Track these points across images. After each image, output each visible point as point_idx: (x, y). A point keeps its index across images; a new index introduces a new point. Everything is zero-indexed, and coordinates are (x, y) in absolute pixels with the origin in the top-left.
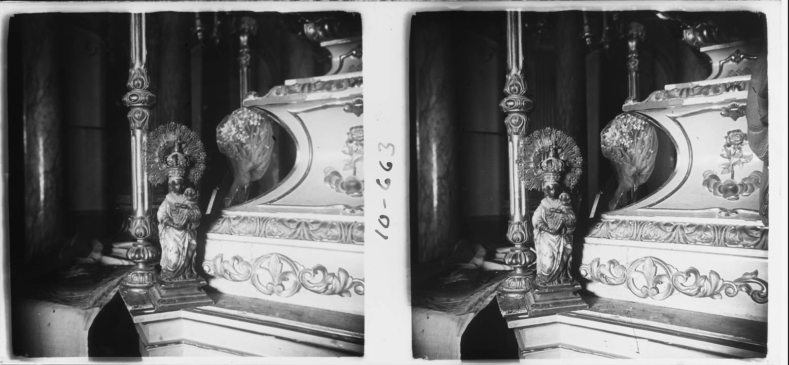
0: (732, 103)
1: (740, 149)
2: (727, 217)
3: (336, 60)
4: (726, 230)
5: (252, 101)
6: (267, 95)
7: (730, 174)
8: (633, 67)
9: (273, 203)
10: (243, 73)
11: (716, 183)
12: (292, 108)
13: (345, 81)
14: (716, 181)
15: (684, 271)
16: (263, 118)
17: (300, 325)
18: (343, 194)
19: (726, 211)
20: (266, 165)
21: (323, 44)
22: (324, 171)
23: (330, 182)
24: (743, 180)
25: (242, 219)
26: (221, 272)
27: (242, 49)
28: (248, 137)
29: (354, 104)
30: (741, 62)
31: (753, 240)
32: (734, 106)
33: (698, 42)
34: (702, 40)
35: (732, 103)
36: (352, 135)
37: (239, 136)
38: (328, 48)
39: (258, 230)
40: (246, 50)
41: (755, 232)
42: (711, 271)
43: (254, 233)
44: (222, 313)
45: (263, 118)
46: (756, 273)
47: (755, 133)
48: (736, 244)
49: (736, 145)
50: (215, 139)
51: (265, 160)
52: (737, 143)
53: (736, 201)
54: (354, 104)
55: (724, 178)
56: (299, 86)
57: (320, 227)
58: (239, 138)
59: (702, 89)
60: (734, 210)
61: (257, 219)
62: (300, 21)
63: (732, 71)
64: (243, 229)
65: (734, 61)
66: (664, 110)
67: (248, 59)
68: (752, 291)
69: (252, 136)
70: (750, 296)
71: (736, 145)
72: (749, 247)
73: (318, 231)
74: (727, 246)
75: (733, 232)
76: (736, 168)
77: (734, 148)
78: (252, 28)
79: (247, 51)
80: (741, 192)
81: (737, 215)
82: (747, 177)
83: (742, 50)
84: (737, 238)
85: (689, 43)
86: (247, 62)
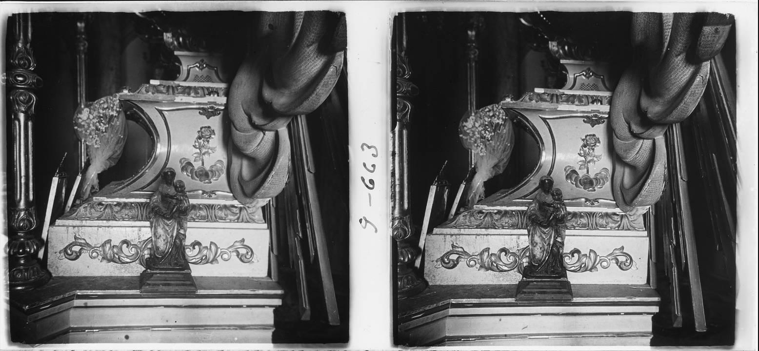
0: (594, 114)
1: (593, 149)
2: (593, 206)
3: (571, 77)
4: (596, 217)
5: (509, 103)
6: (521, 99)
7: (586, 170)
8: (472, 56)
9: (527, 198)
10: (471, 67)
11: (576, 177)
12: (543, 114)
13: (584, 97)
14: (576, 176)
15: (569, 252)
16: (507, 118)
17: (581, 300)
18: (582, 189)
19: (590, 201)
20: (507, 162)
21: (562, 61)
22: (565, 170)
23: (571, 179)
24: (595, 175)
25: (503, 213)
26: (488, 264)
27: (469, 43)
28: (493, 134)
29: (592, 117)
30: (590, 78)
31: (616, 224)
32: (595, 116)
33: (560, 55)
34: (563, 53)
35: (594, 114)
36: (587, 141)
37: (485, 133)
38: (565, 65)
39: (520, 222)
40: (474, 44)
41: (616, 217)
42: (590, 250)
43: (517, 226)
44: (496, 303)
45: (507, 118)
46: (623, 248)
47: (623, 142)
48: (604, 227)
49: (590, 146)
50: (458, 133)
51: (506, 157)
52: (592, 145)
53: (593, 192)
54: (592, 117)
55: (582, 173)
56: (548, 95)
57: (572, 218)
58: (485, 135)
59: (569, 97)
60: (596, 199)
61: (518, 213)
62: (539, 35)
63: (583, 84)
64: (506, 223)
65: (585, 76)
66: (539, 112)
67: (476, 55)
68: (620, 262)
69: (496, 133)
70: (618, 267)
71: (590, 146)
72: (611, 229)
73: (571, 221)
74: (598, 229)
75: (601, 218)
76: (591, 165)
77: (589, 149)
78: (480, 25)
79: (474, 46)
80: (596, 185)
81: (599, 204)
82: (598, 172)
83: (592, 69)
84: (604, 223)
85: (552, 53)
86: (475, 57)
